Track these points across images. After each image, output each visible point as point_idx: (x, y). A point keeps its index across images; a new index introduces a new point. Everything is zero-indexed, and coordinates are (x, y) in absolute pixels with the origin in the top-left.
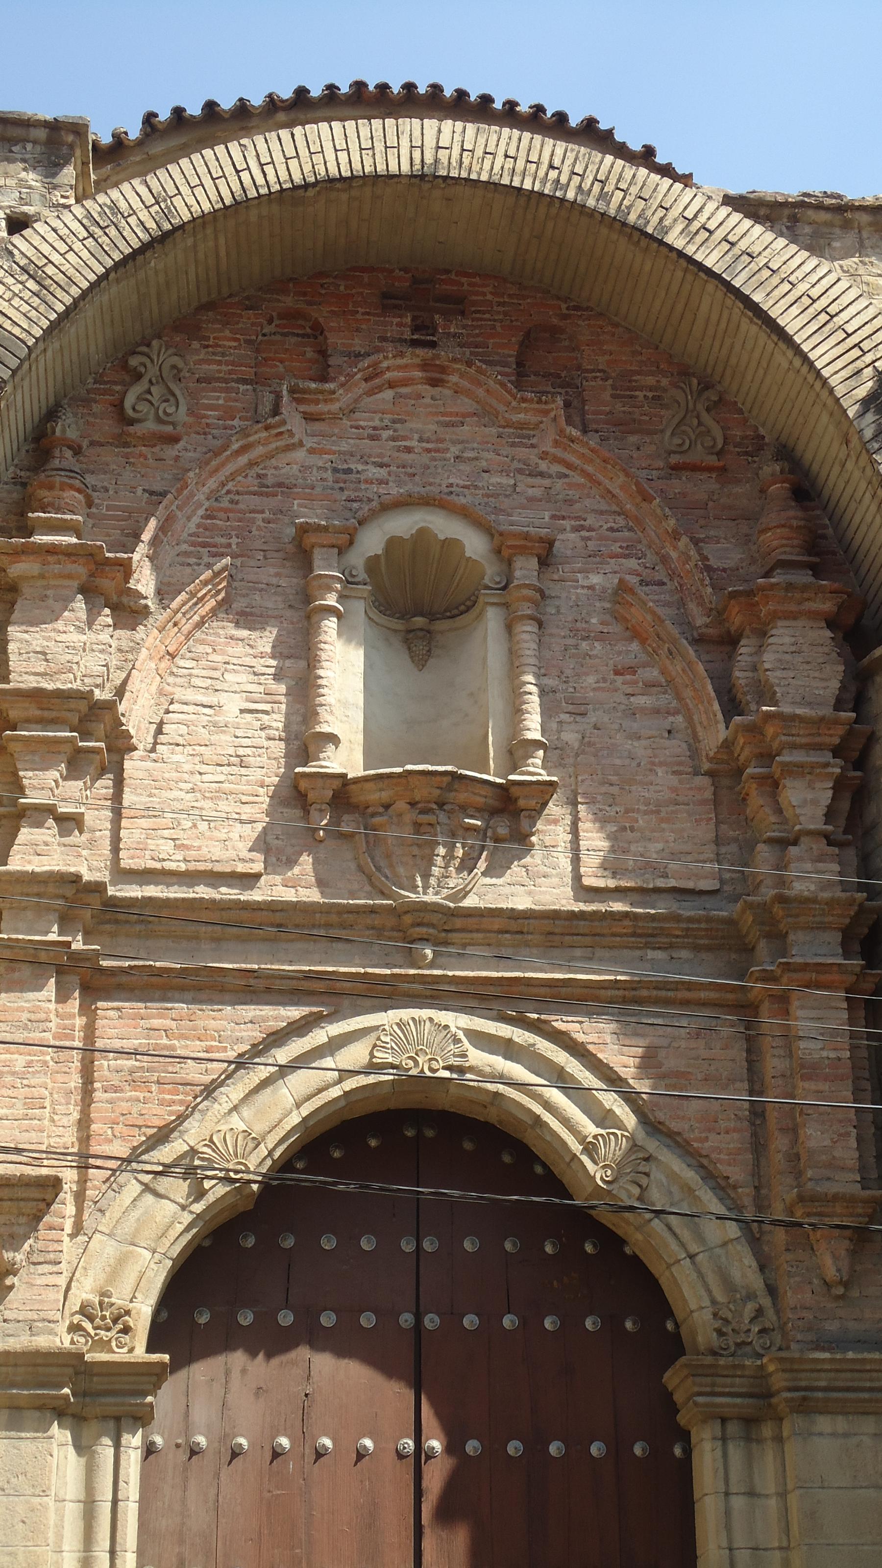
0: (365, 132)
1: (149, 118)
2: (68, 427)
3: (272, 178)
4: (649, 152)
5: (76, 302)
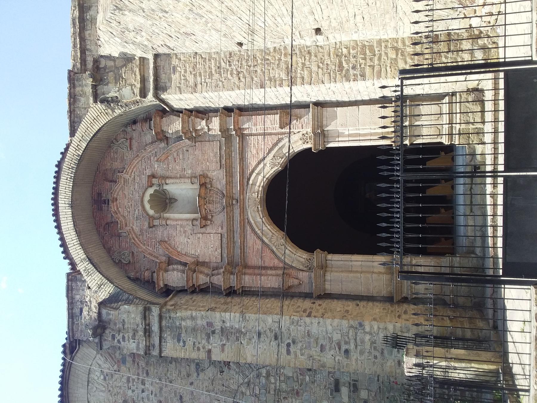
0: (63, 219)
1: (65, 258)
2: (132, 275)
3: (75, 238)
4: (62, 153)
5: (105, 278)
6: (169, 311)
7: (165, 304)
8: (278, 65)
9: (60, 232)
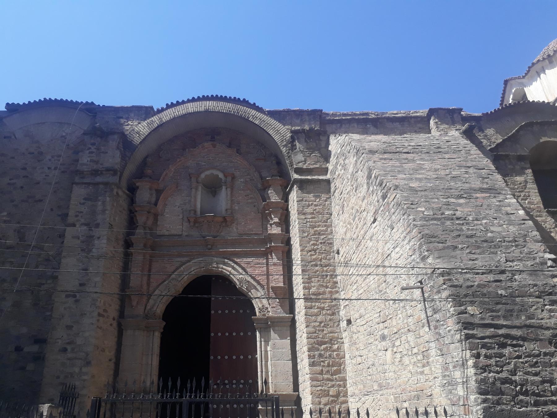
1: (167, 104)
2: (149, 160)
4: (254, 104)
5: (145, 137)
6: (112, 190)
7: (119, 187)
8: (322, 285)
9: (189, 101)
